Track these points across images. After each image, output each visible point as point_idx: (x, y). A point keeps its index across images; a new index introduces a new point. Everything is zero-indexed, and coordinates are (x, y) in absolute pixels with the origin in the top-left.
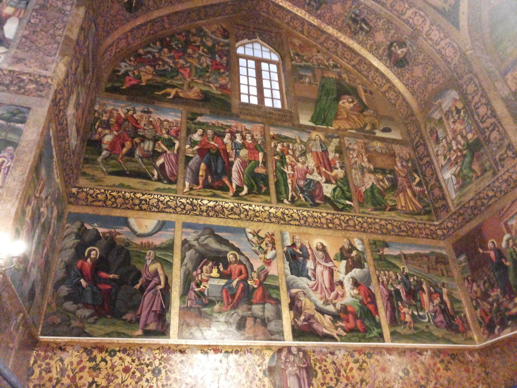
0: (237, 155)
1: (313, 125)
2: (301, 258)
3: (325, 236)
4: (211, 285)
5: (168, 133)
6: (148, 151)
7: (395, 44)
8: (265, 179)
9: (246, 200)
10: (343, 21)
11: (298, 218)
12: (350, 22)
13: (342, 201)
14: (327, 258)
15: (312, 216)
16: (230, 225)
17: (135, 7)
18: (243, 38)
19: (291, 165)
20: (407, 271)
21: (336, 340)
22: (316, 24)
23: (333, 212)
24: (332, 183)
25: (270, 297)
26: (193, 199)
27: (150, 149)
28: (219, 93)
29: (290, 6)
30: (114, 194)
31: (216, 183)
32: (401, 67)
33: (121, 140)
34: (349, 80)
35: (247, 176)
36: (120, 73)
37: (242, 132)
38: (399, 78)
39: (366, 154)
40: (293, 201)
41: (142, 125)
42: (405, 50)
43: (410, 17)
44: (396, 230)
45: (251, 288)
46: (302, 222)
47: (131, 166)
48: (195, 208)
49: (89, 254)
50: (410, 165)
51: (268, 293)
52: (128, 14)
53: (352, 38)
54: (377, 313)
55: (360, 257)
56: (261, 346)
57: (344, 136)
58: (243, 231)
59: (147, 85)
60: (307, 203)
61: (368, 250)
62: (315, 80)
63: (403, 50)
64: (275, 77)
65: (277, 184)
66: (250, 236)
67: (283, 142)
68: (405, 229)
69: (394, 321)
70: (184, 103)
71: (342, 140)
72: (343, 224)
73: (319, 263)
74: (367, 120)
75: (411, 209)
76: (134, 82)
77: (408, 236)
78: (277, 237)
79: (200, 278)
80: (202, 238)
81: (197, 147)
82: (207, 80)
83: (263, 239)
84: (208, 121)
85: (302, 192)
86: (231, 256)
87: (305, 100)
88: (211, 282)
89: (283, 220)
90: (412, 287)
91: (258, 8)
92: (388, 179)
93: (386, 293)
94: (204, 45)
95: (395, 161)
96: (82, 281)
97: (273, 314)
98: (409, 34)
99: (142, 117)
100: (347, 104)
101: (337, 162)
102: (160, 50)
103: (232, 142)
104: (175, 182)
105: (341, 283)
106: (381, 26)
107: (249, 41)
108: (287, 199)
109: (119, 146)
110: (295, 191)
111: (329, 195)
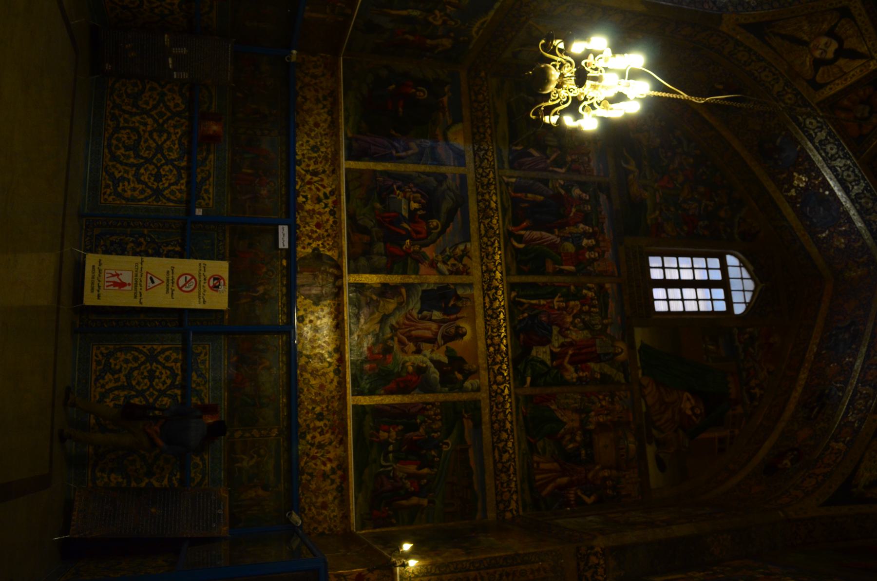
0: (566, 239)
3: (475, 338)
4: (400, 201)
5: (573, 161)
7: (796, 453)
8: (540, 270)
14: (448, 338)
19: (567, 307)
20: (445, 449)
24: (552, 360)
30: (486, 109)
44: (501, 445)
46: (490, 312)
49: (421, 91)
50: (609, 492)
58: (467, 238)
60: (516, 322)
61: (464, 397)
63: (789, 464)
64: (705, 307)
65: (533, 285)
66: (462, 247)
68: (504, 460)
69: (378, 411)
72: (496, 367)
73: (439, 327)
75: (538, 477)
77: (495, 463)
78: (465, 279)
80: (451, 194)
81: (563, 192)
86: (435, 224)
89: (488, 287)
90: (424, 451)
96: (394, 86)
105: (418, 351)
108: (518, 296)
111: (534, 353)
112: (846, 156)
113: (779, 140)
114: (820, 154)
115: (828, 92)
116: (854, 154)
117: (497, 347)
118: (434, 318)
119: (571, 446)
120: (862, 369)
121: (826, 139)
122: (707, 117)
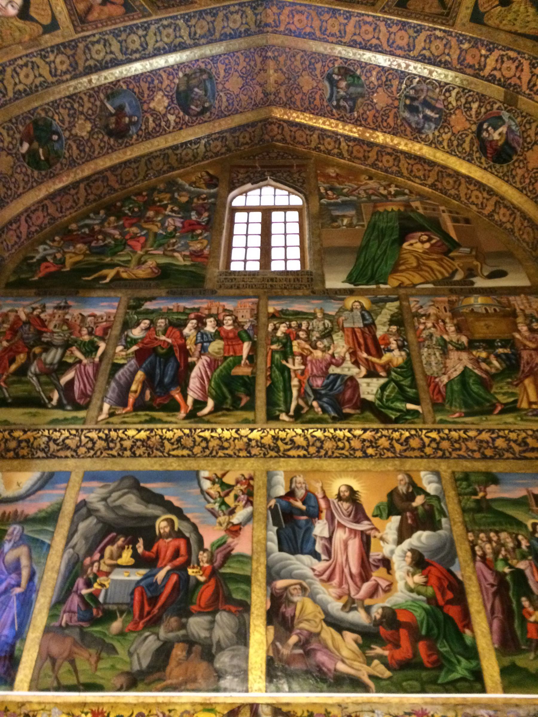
0: (204, 351)
1: (351, 286)
2: (304, 518)
3: (357, 473)
4: (115, 582)
5: (90, 333)
6: (51, 364)
7: (485, 126)
8: (249, 384)
9: (208, 422)
10: (396, 117)
11: (304, 443)
12: (406, 114)
13: (398, 405)
14: (359, 514)
16: (171, 468)
17: (47, 160)
18: (243, 184)
19: (301, 355)
22: (356, 135)
23: (375, 426)
24: (378, 376)
25: (229, 599)
26: (110, 430)
27: (56, 361)
28: (188, 263)
29: (311, 119)
31: (158, 401)
32: (505, 161)
33: (11, 353)
34: (425, 209)
35: (217, 384)
36: (35, 260)
37: (218, 314)
38: (507, 181)
39: (452, 318)
40: (298, 416)
41: (51, 327)
42: (503, 129)
43: (495, 69)
44: (517, 448)
45: (192, 582)
46: (312, 450)
47: (18, 390)
48: (111, 445)
52: (36, 173)
53: (415, 139)
54: (468, 624)
55: (431, 506)
56: (193, 704)
59: (72, 270)
60: (326, 416)
61: (451, 493)
62: (361, 219)
63: (500, 130)
65: (270, 391)
66: (206, 485)
67: (290, 321)
70: (126, 286)
71: (405, 303)
73: (340, 525)
74: (456, 264)
76: (53, 269)
78: (259, 484)
79: (95, 569)
80: (115, 495)
81: (135, 348)
82: (171, 248)
83: (231, 487)
84: (162, 307)
85: (318, 396)
86: (164, 524)
87: (340, 251)
88: (118, 576)
91: (266, 137)
92: (498, 356)
93: (491, 579)
94: (173, 200)
95: (515, 324)
97: (229, 633)
98: (502, 98)
99: (53, 315)
100: (419, 245)
101: (392, 340)
102: (103, 221)
103: (199, 331)
104: (86, 407)
105: (386, 563)
106: (454, 104)
108: (287, 412)
109: (6, 361)
110: (303, 399)
111: (370, 398)
112: (146, 27)
113: (109, 106)
114: (137, 60)
115: (63, 17)
116: (144, 16)
117: (367, 444)
118: (326, 534)
119: (496, 363)
120: (392, 54)
121: (120, 42)
122: (59, 185)
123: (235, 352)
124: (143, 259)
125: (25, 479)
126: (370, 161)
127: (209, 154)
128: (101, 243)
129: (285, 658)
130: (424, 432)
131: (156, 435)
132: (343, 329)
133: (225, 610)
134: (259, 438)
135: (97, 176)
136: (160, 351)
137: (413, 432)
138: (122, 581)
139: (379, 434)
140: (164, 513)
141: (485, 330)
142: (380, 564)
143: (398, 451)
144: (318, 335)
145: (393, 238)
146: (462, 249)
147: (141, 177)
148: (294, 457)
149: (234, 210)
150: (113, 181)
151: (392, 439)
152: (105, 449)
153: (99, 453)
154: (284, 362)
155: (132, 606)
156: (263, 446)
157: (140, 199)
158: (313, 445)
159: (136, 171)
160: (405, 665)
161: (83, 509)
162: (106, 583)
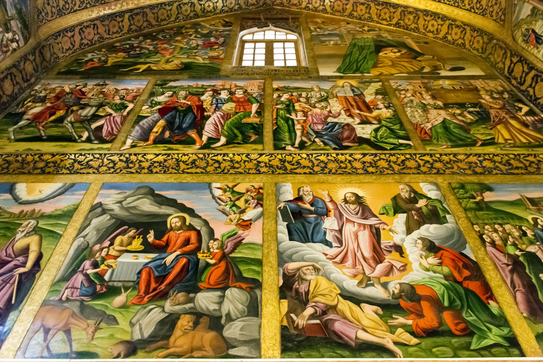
1: (342, 75)
6: (85, 116)
11: (310, 165)
15: (336, 161)
18: (251, 27)
21: (392, 354)
24: (371, 123)
25: (240, 278)
26: (130, 155)
31: (176, 138)
45: (201, 264)
47: (54, 131)
48: (131, 165)
51: (234, 272)
57: (388, 81)
59: (112, 66)
60: (328, 147)
65: (276, 133)
72: (396, 168)
79: (104, 253)
80: (129, 200)
83: (241, 194)
88: (127, 258)
92: (470, 113)
97: (240, 307)
101: (379, 103)
105: (399, 249)
107: (260, 29)
108: (293, 145)
110: (305, 137)
123: (245, 109)
124: (170, 60)
125: (48, 188)
126: (347, 13)
127: (226, 9)
128: (138, 52)
129: (300, 327)
130: (418, 156)
131: (172, 158)
132: (337, 97)
133: (235, 287)
134: (267, 161)
135: (139, 11)
136: (180, 108)
137: (408, 156)
138: (129, 263)
139: (378, 158)
140: (176, 212)
141: (455, 98)
142: (393, 250)
143: (396, 170)
144: (316, 100)
145: (370, 50)
146: (425, 56)
147: (173, 19)
148: (300, 174)
149: (243, 42)
150: (151, 17)
151: (390, 161)
152: (125, 168)
153: (118, 171)
154: (288, 115)
155: (138, 283)
156: (271, 166)
157: (172, 31)
158: (318, 165)
159: (169, 12)
160: (431, 333)
161: (98, 209)
162: (113, 265)
